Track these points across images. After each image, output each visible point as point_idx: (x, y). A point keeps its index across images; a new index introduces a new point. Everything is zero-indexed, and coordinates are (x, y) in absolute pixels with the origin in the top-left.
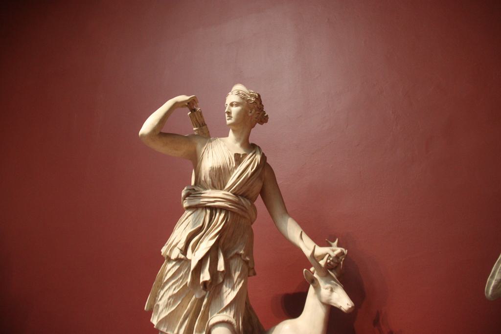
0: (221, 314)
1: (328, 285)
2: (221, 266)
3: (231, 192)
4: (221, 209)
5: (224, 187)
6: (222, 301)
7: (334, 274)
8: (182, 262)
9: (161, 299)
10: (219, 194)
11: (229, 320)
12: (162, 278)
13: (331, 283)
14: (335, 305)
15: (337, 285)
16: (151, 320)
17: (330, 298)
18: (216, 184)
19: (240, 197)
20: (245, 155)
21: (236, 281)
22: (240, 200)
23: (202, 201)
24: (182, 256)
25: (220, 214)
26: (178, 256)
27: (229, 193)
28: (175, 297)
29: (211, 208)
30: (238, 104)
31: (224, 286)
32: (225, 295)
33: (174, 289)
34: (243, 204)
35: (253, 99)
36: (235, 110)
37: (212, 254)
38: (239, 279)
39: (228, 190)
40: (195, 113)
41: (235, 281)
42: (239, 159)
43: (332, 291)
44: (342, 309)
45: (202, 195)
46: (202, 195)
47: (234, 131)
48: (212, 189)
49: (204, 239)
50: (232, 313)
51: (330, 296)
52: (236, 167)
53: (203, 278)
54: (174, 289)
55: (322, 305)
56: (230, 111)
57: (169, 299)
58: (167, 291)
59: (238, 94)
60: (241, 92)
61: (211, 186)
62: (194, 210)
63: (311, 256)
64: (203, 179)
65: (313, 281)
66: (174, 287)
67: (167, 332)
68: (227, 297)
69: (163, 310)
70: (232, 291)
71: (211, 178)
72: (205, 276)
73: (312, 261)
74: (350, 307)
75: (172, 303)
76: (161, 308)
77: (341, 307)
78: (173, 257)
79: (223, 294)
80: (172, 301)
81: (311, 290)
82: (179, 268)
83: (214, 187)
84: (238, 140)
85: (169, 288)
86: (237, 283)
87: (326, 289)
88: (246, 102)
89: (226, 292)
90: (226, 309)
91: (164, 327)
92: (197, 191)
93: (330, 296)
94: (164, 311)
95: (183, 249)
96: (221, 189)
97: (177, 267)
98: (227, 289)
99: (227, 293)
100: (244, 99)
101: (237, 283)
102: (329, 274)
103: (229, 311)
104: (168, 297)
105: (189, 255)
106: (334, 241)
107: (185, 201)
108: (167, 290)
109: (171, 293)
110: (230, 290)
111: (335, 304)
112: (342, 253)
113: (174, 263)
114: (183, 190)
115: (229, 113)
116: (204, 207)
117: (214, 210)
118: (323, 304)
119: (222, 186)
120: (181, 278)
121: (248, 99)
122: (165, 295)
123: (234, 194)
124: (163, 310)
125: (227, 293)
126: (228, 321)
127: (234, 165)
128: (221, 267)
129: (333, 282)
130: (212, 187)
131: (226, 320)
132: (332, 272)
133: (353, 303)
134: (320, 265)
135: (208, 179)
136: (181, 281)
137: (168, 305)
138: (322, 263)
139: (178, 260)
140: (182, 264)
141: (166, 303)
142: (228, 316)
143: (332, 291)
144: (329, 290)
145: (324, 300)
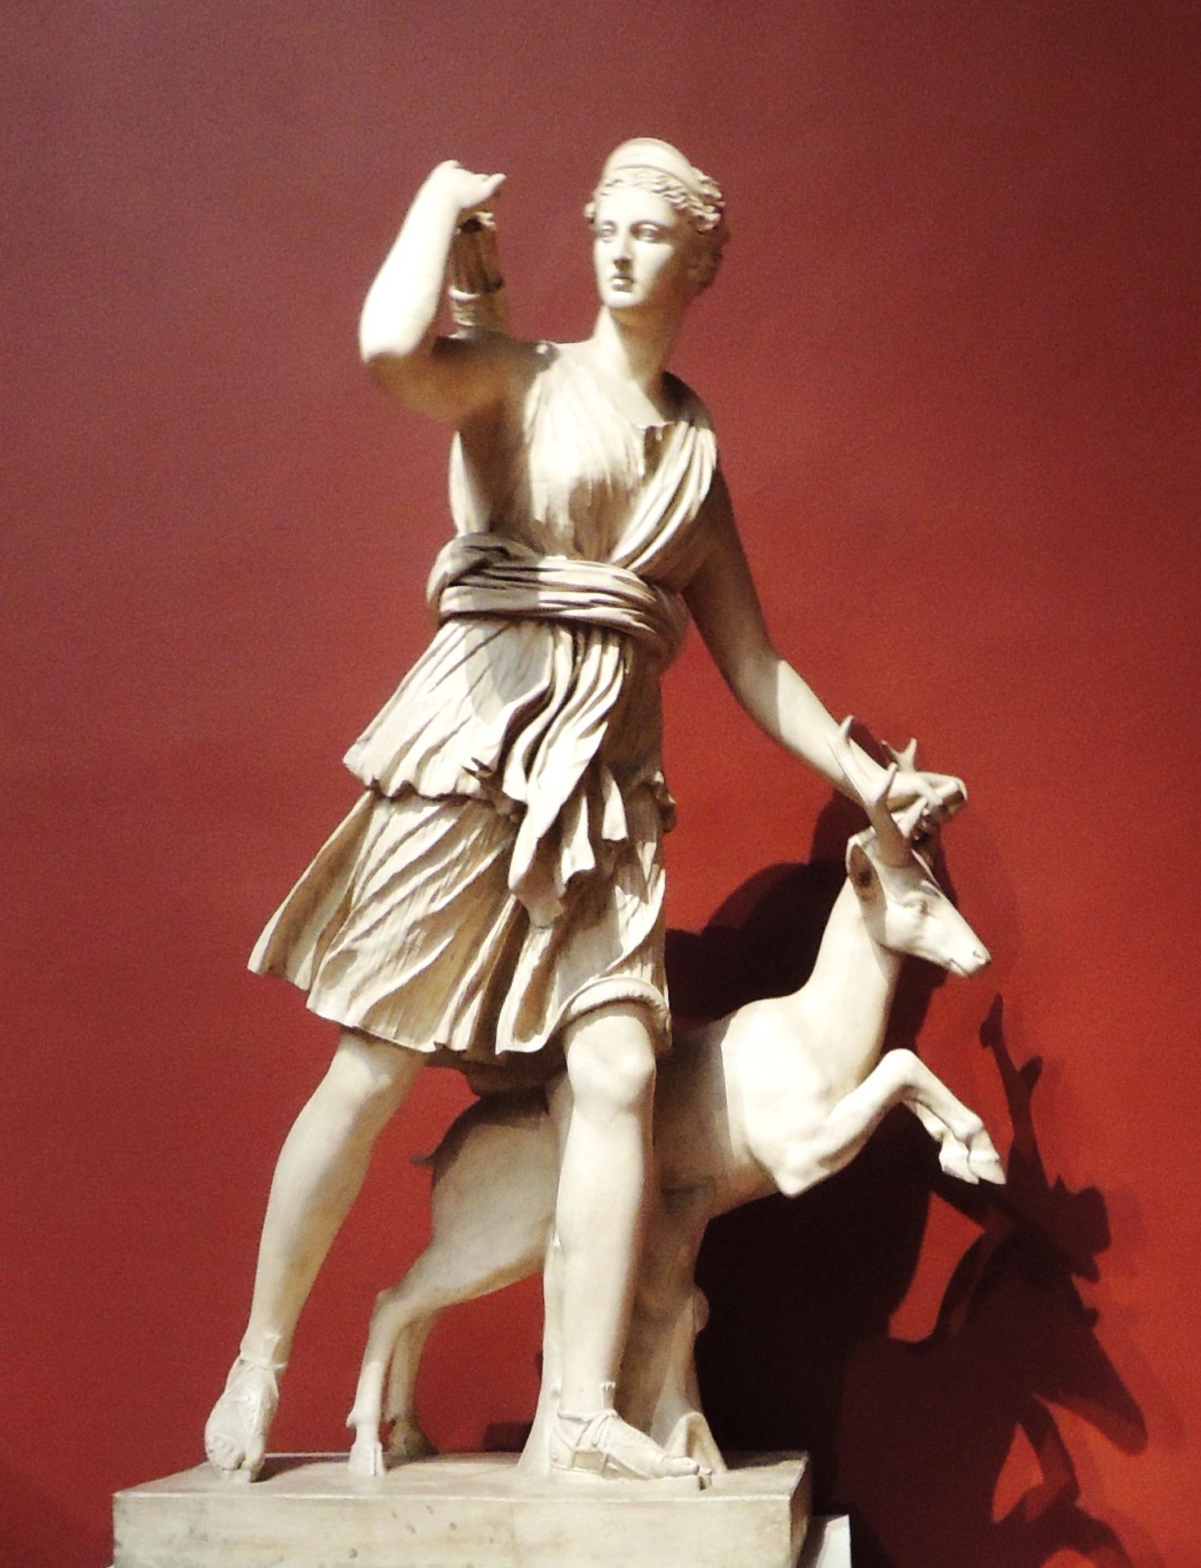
0: (616, 976)
1: (915, 896)
2: (615, 825)
3: (635, 572)
4: (608, 631)
6: (613, 935)
7: (925, 859)
8: (465, 807)
9: (368, 933)
10: (604, 575)
11: (646, 994)
13: (924, 890)
14: (930, 957)
15: (936, 895)
16: (310, 1005)
17: (918, 933)
18: (586, 545)
19: (655, 586)
20: (667, 431)
21: (650, 876)
22: (659, 600)
23: (545, 598)
25: (604, 650)
28: (433, 924)
30: (660, 234)
31: (618, 889)
32: (622, 918)
33: (433, 900)
34: (665, 612)
35: (713, 217)
36: (650, 256)
37: (590, 786)
38: (656, 866)
39: (618, 564)
40: (479, 234)
41: (646, 872)
42: (653, 449)
43: (924, 911)
44: (954, 968)
45: (542, 576)
46: (542, 576)
47: (625, 329)
48: (570, 556)
50: (649, 969)
51: (918, 927)
52: (645, 480)
53: (573, 863)
54: (433, 900)
55: (878, 949)
56: (629, 256)
57: (410, 930)
58: (407, 902)
60: (673, 183)
61: (570, 544)
63: (879, 801)
64: (539, 515)
65: (865, 878)
66: (431, 890)
67: (395, 1041)
68: (627, 923)
69: (380, 968)
70: (643, 904)
71: (573, 515)
72: (577, 857)
73: (872, 814)
74: (982, 961)
75: (419, 943)
77: (952, 960)
78: (435, 782)
79: (616, 912)
80: (421, 937)
81: (848, 903)
82: (453, 827)
83: (578, 549)
84: (637, 367)
85: (413, 894)
86: (652, 879)
87: (908, 905)
88: (688, 228)
89: (625, 906)
90: (629, 962)
91: (388, 1023)
92: (517, 558)
93: (918, 927)
94: (385, 972)
95: (494, 767)
96: (603, 554)
97: (444, 825)
98: (628, 897)
99: (629, 910)
100: (681, 213)
101: (652, 879)
102: (914, 858)
103: (639, 965)
104: (408, 921)
105: (514, 785)
106: (902, 748)
107: (454, 590)
108: (403, 900)
109: (420, 909)
110: (637, 899)
111: (930, 951)
112: (957, 797)
113: (430, 810)
114: (446, 552)
115: (624, 265)
116: (549, 620)
117: (585, 631)
118: (887, 950)
120: (458, 859)
121: (699, 213)
122: (390, 919)
123: (642, 577)
124: (380, 968)
125: (629, 910)
126: (641, 996)
127: (641, 470)
128: (615, 828)
129: (925, 883)
130: (572, 550)
131: (637, 995)
132: (919, 853)
133: (988, 955)
134: (895, 827)
135: (563, 521)
136: (457, 869)
137: (403, 952)
138: (905, 821)
139: (452, 800)
140: (467, 810)
141: (396, 947)
142: (640, 981)
143: (924, 911)
144: (918, 908)
145: (893, 940)
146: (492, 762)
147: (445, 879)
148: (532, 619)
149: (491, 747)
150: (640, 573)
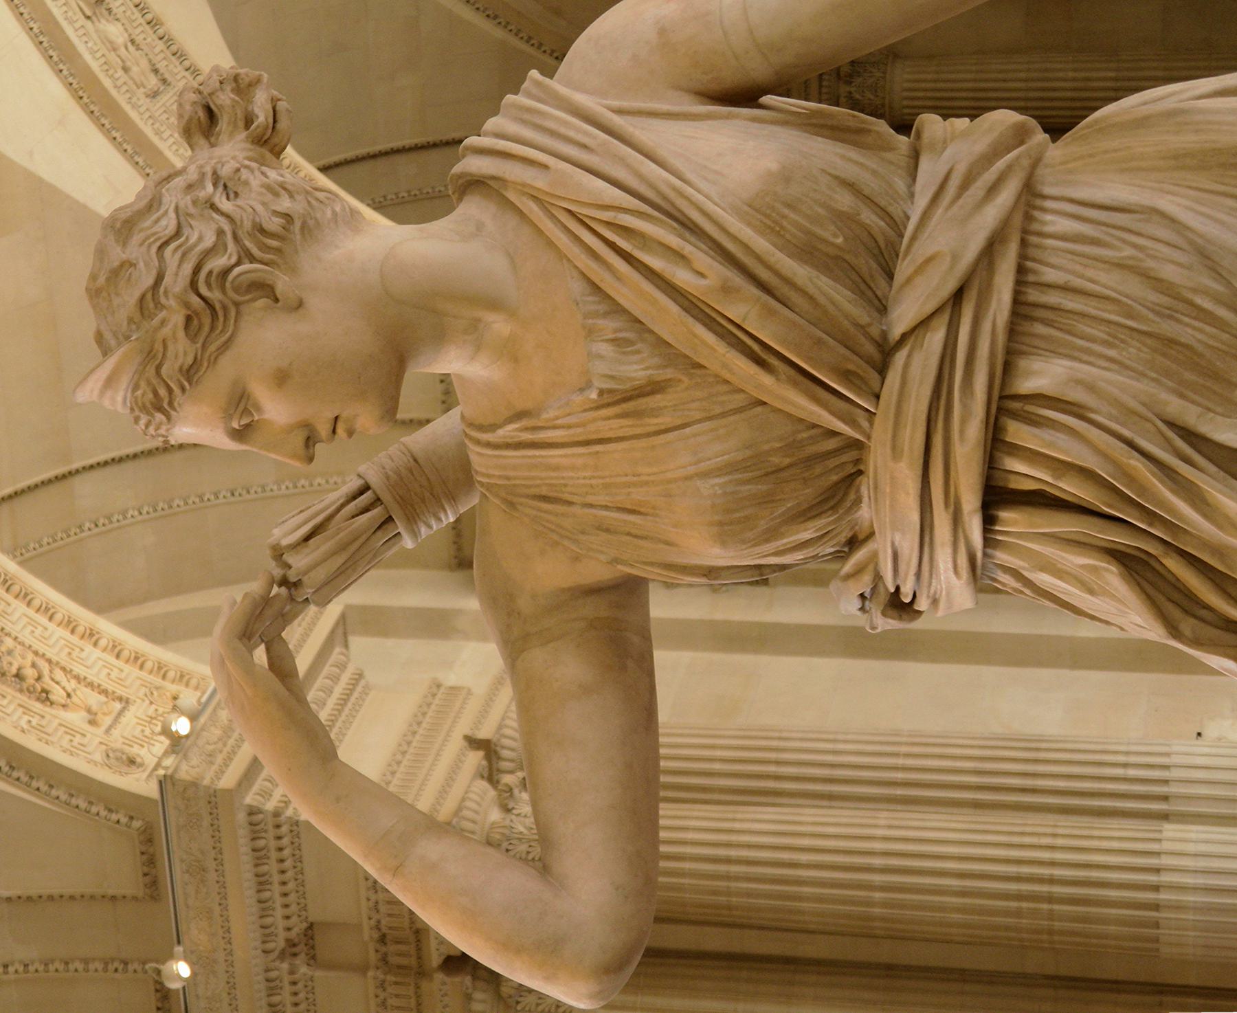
119: (832, 444)
150: (873, 376)
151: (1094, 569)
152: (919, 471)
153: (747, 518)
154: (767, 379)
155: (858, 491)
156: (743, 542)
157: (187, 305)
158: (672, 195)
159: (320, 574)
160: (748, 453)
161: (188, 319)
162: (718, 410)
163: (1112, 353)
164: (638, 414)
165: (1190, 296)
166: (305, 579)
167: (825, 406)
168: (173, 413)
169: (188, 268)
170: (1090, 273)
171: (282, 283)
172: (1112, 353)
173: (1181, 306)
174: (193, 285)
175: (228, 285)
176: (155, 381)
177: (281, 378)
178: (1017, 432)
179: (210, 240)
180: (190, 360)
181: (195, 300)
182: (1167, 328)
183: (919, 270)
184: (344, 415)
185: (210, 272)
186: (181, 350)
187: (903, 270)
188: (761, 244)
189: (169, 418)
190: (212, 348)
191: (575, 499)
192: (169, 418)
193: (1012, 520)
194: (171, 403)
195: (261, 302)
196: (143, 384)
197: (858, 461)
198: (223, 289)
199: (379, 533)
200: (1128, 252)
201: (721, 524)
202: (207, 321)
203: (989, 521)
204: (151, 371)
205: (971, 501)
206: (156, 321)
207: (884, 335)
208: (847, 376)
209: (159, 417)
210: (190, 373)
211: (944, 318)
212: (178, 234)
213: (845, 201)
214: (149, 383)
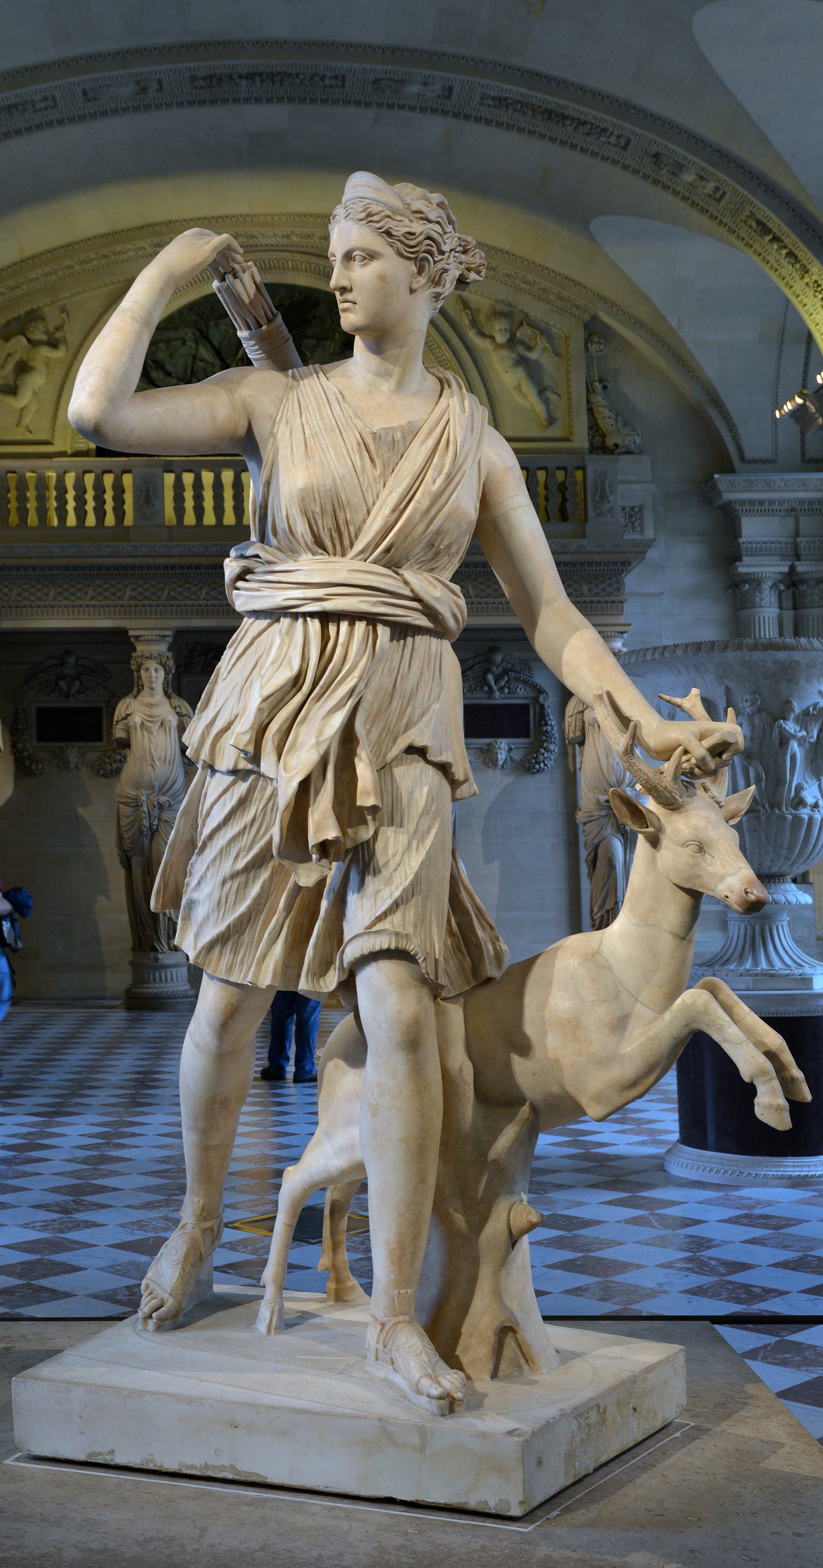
5: (352, 545)
12: (194, 820)
24: (243, 765)
26: (236, 764)
27: (368, 566)
29: (326, 618)
49: (308, 712)
57: (224, 882)
58: (218, 862)
59: (369, 217)
62: (268, 621)
75: (232, 897)
76: (200, 912)
94: (213, 918)
95: (251, 749)
104: (220, 878)
105: (267, 765)
109: (227, 868)
119: (347, 542)
146: (247, 744)
147: (244, 841)
148: (286, 615)
149: (244, 733)
151: (290, 663)
152: (343, 582)
153: (315, 501)
154: (387, 510)
155: (321, 554)
156: (303, 499)
157: (421, 234)
158: (462, 470)
159: (240, 288)
160: (345, 502)
161: (413, 234)
162: (364, 489)
163: (386, 671)
164: (360, 451)
165: (411, 704)
166: (238, 281)
167: (373, 539)
168: (365, 222)
169: (436, 236)
170: (418, 660)
171: (422, 280)
172: (386, 671)
173: (406, 700)
174: (429, 238)
175: (426, 255)
176: (383, 214)
177: (382, 278)
178: (360, 627)
179: (446, 248)
180: (394, 233)
181: (421, 238)
182: (397, 696)
183: (431, 583)
184: (357, 306)
185: (432, 246)
186: (400, 230)
187: (427, 575)
188: (446, 509)
189: (362, 220)
190: (399, 244)
191: (304, 420)
192: (362, 220)
193: (314, 626)
194: (371, 221)
195: (415, 270)
196: (380, 209)
197: (335, 555)
198: (425, 252)
199: (254, 320)
200: (427, 677)
201: (313, 488)
202: (412, 243)
203: (312, 615)
204: (389, 213)
205: (328, 606)
206: (412, 217)
207: (400, 567)
208: (388, 550)
209: (363, 215)
210: (388, 233)
211: (410, 594)
212: (445, 233)
213: (454, 549)
214: (381, 211)
